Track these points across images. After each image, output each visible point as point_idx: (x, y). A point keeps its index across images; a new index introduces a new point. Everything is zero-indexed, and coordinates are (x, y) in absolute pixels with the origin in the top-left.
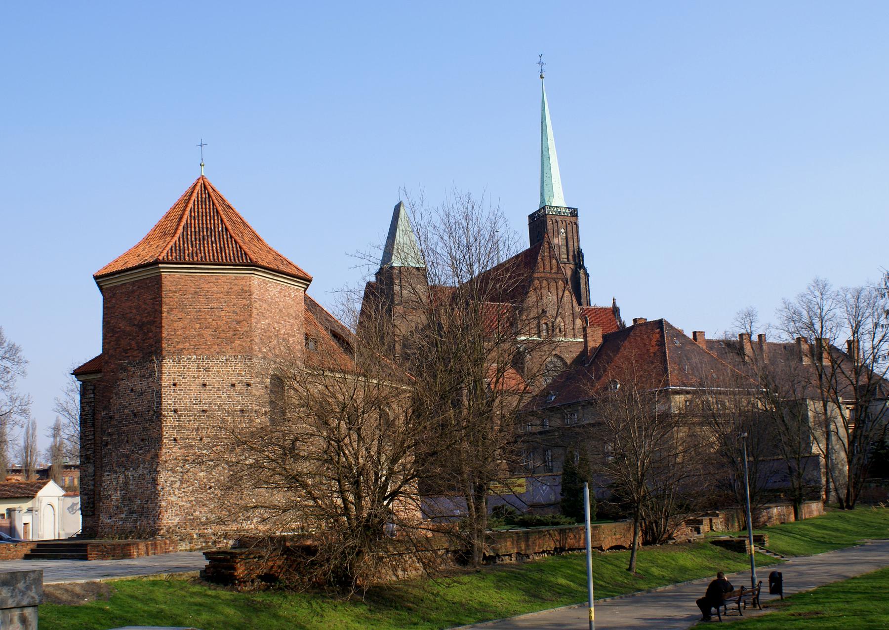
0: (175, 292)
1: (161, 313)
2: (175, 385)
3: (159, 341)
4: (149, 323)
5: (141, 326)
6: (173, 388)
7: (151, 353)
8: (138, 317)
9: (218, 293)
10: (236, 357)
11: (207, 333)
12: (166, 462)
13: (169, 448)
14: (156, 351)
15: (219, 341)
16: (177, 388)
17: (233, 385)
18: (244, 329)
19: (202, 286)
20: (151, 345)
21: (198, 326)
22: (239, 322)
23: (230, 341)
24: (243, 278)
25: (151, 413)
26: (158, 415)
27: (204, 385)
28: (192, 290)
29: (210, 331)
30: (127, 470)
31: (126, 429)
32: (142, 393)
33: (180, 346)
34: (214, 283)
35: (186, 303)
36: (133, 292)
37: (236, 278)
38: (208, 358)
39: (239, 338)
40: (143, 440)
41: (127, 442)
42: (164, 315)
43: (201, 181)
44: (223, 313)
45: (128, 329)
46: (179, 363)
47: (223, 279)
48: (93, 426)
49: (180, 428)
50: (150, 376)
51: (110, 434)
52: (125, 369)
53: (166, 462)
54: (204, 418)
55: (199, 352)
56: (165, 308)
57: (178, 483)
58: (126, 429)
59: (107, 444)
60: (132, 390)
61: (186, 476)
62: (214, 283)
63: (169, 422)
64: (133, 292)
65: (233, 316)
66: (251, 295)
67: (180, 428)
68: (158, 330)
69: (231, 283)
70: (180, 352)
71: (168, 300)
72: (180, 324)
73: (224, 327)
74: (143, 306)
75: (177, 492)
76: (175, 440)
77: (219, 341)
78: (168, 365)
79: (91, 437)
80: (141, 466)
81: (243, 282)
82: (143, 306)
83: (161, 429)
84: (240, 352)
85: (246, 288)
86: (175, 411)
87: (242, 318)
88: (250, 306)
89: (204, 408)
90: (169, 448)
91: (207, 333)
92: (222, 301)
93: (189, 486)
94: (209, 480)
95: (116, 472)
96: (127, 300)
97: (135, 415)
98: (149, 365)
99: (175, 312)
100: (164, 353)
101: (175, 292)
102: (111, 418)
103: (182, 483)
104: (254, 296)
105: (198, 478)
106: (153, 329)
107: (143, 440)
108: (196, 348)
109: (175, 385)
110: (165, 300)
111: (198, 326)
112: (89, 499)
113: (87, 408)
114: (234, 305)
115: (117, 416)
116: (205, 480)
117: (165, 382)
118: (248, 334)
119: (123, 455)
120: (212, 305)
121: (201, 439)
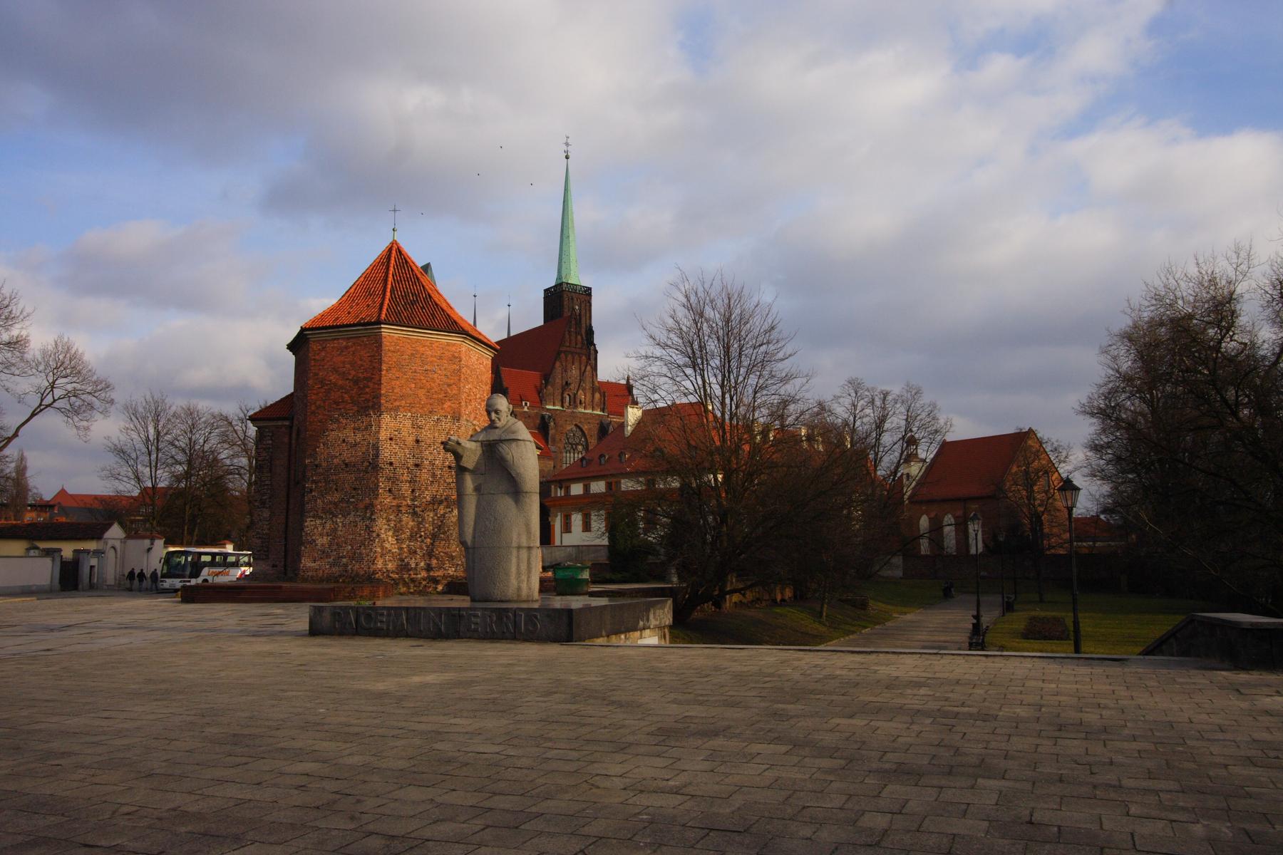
1: (381, 370)
3: (378, 396)
4: (365, 378)
5: (356, 382)
7: (366, 408)
8: (353, 373)
10: (446, 417)
20: (368, 401)
22: (449, 385)
23: (441, 402)
25: (366, 464)
27: (417, 441)
28: (409, 352)
29: (423, 391)
33: (397, 403)
50: (366, 429)
51: (313, 482)
56: (384, 367)
59: (311, 491)
64: (346, 347)
65: (444, 379)
70: (396, 409)
71: (388, 358)
78: (386, 419)
88: (459, 370)
91: (421, 393)
97: (346, 465)
100: (383, 408)
106: (371, 385)
108: (411, 406)
110: (385, 359)
115: (324, 464)
117: (383, 435)
118: (456, 398)
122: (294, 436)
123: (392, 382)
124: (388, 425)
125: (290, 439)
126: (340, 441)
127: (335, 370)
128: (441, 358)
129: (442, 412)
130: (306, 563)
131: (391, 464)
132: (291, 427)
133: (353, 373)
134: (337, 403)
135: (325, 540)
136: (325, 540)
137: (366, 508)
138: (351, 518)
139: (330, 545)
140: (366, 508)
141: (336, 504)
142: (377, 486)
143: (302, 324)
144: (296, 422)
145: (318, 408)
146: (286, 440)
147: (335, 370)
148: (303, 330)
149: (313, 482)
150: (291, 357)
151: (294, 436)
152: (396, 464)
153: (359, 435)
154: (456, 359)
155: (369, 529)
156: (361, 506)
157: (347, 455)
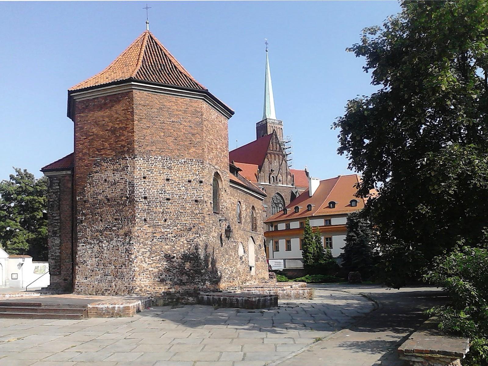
0: (144, 106)
3: (131, 143)
6: (143, 180)
7: (123, 153)
9: (177, 110)
11: (170, 140)
12: (138, 236)
16: (147, 180)
17: (190, 181)
19: (165, 104)
20: (124, 147)
21: (162, 134)
22: (193, 135)
26: (132, 200)
27: (168, 180)
28: (158, 106)
32: (115, 184)
33: (149, 148)
34: (174, 102)
35: (153, 115)
38: (170, 159)
39: (194, 146)
40: (116, 219)
42: (136, 123)
44: (181, 126)
46: (148, 161)
47: (181, 100)
50: (123, 170)
53: (138, 236)
55: (163, 155)
56: (136, 117)
57: (148, 253)
61: (154, 248)
62: (174, 102)
63: (141, 206)
66: (202, 115)
68: (130, 134)
69: (187, 105)
72: (149, 131)
73: (182, 137)
75: (147, 260)
76: (145, 220)
77: (178, 147)
78: (140, 162)
81: (196, 105)
83: (134, 211)
85: (198, 110)
86: (145, 198)
88: (202, 123)
89: (168, 197)
90: (140, 226)
91: (170, 140)
92: (181, 117)
93: (156, 256)
98: (122, 162)
99: (144, 121)
100: (136, 152)
101: (144, 106)
103: (151, 253)
105: (163, 249)
106: (125, 133)
108: (161, 151)
109: (144, 178)
111: (162, 134)
114: (189, 121)
117: (137, 174)
120: (173, 119)
121: (165, 221)
123: (142, 131)
124: (140, 166)
126: (102, 182)
129: (187, 156)
131: (145, 198)
137: (126, 235)
138: (114, 243)
142: (134, 217)
145: (85, 154)
147: (96, 123)
149: (83, 214)
152: (150, 198)
153: (117, 177)
154: (197, 113)
155: (128, 252)
156: (121, 232)
157: (109, 193)
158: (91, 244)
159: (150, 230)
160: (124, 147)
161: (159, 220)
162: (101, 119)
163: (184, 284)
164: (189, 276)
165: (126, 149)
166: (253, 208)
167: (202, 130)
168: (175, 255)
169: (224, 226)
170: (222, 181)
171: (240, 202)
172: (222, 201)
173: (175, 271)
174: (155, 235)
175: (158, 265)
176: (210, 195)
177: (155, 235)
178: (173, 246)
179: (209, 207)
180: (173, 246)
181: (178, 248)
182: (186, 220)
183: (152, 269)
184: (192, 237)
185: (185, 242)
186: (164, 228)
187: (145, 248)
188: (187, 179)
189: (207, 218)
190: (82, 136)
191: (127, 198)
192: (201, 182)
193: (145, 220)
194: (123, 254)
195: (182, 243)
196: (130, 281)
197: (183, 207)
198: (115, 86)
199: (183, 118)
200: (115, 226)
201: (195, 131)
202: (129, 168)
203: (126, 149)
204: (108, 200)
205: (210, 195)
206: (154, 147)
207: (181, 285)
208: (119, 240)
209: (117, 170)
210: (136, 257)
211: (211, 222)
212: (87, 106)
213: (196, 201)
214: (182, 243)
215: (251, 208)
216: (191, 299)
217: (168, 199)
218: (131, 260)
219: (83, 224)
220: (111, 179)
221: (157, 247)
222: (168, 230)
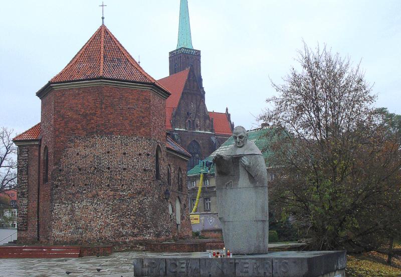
2: (108, 152)
4: (91, 114)
7: (92, 133)
8: (83, 110)
13: (105, 191)
14: (97, 132)
15: (133, 128)
17: (140, 155)
18: (146, 122)
20: (94, 128)
22: (143, 118)
24: (145, 92)
25: (93, 168)
27: (124, 154)
30: (75, 203)
31: (72, 177)
33: (111, 130)
36: (79, 94)
37: (142, 91)
40: (86, 185)
41: (74, 185)
43: (103, 28)
44: (135, 111)
45: (75, 117)
48: (27, 174)
49: (111, 179)
51: (59, 180)
52: (72, 141)
53: (103, 198)
54: (125, 173)
57: (110, 211)
58: (72, 177)
59: (57, 186)
60: (78, 154)
64: (79, 94)
66: (150, 102)
67: (111, 179)
70: (111, 133)
74: (87, 104)
77: (133, 128)
79: (25, 181)
80: (85, 200)
81: (145, 94)
82: (87, 104)
84: (144, 135)
86: (109, 168)
87: (145, 115)
92: (135, 104)
93: (116, 213)
94: (127, 210)
95: (65, 204)
96: (73, 99)
97: (80, 170)
99: (109, 109)
102: (60, 170)
104: (151, 103)
106: (95, 118)
107: (86, 185)
109: (108, 152)
112: (23, 220)
113: (23, 163)
115: (65, 169)
116: (125, 210)
119: (70, 194)
121: (123, 185)
122: (42, 151)
125: (39, 154)
127: (71, 108)
128: (138, 100)
130: (56, 232)
131: (109, 168)
132: (40, 146)
133: (83, 110)
134: (73, 130)
135: (66, 218)
136: (66, 218)
137: (94, 197)
138: (84, 203)
139: (71, 220)
140: (94, 197)
141: (73, 194)
143: (50, 79)
144: (43, 142)
146: (37, 154)
147: (71, 108)
148: (50, 83)
150: (38, 101)
151: (42, 151)
153: (88, 151)
154: (147, 100)
156: (90, 195)
157: (80, 164)
158: (65, 204)
159: (112, 193)
160: (94, 128)
161: (119, 185)
162: (75, 106)
163: (136, 236)
164: (139, 229)
165: (95, 130)
166: (180, 169)
167: (150, 114)
168: (129, 213)
169: (164, 188)
170: (161, 152)
171: (169, 165)
172: (161, 168)
173: (129, 226)
174: (115, 197)
175: (117, 221)
176: (154, 164)
177: (115, 197)
178: (128, 206)
179: (153, 175)
180: (128, 206)
181: (132, 207)
182: (138, 185)
183: (113, 224)
184: (141, 199)
185: (137, 202)
186: (122, 191)
187: (108, 208)
188: (138, 153)
189: (152, 184)
190: (59, 118)
191: (95, 168)
192: (148, 155)
193: (108, 185)
194: (92, 212)
195: (134, 204)
196: (98, 232)
197: (136, 175)
198: (88, 81)
199: (136, 105)
200: (85, 190)
201: (145, 115)
202: (97, 146)
203: (95, 130)
204: (80, 170)
205: (154, 164)
206: (116, 128)
207: (133, 236)
208: (89, 200)
209: (87, 146)
210: (102, 214)
211: (155, 186)
212: (63, 95)
213: (145, 170)
214: (134, 204)
215: (178, 170)
216: (141, 247)
217: (125, 169)
218: (98, 216)
219: (59, 188)
220: (83, 153)
221: (117, 206)
222: (124, 193)
